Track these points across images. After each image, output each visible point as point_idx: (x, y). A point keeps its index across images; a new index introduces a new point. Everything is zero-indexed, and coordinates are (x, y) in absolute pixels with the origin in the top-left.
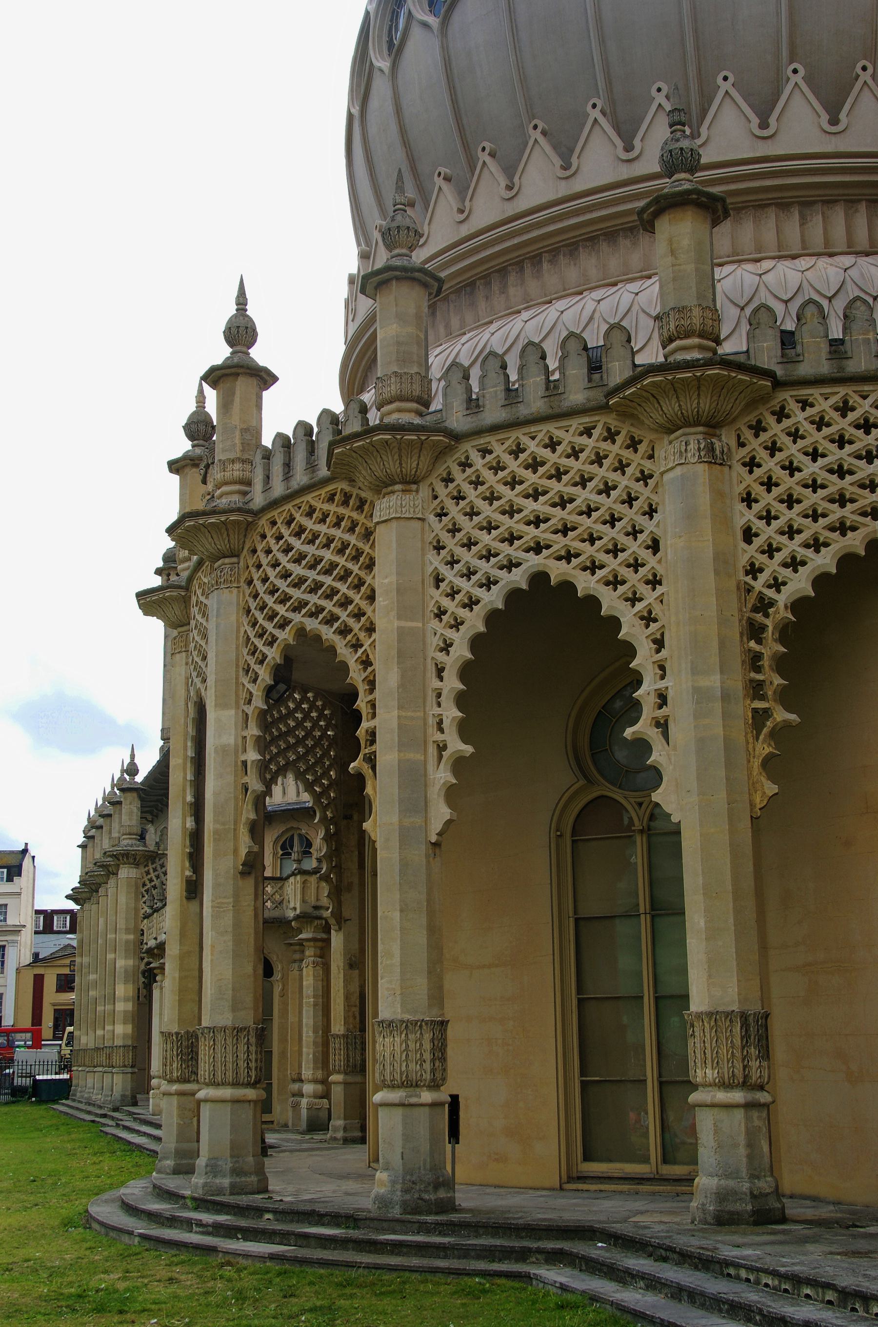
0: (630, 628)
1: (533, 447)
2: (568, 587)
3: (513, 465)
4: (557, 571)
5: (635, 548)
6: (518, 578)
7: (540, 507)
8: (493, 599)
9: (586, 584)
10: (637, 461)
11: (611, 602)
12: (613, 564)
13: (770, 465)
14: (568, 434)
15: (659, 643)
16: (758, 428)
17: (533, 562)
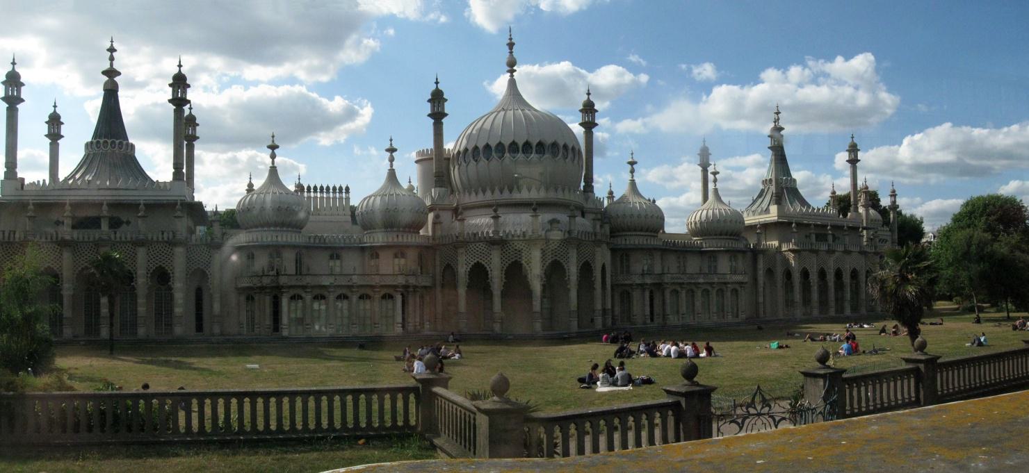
0: (488, 269)
1: (477, 245)
2: (481, 263)
3: (475, 247)
4: (480, 261)
5: (489, 259)
6: (475, 261)
7: (478, 253)
8: (472, 263)
9: (483, 263)
10: (489, 248)
11: (486, 265)
12: (486, 261)
13: (504, 250)
14: (481, 244)
15: (491, 270)
16: (503, 246)
17: (477, 259)
